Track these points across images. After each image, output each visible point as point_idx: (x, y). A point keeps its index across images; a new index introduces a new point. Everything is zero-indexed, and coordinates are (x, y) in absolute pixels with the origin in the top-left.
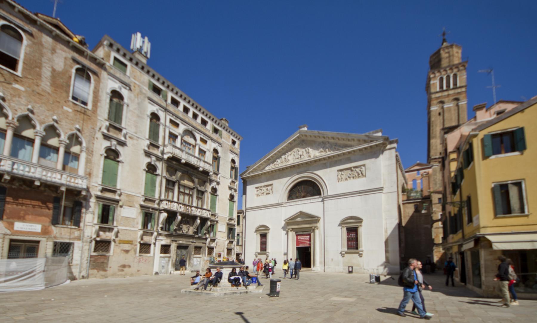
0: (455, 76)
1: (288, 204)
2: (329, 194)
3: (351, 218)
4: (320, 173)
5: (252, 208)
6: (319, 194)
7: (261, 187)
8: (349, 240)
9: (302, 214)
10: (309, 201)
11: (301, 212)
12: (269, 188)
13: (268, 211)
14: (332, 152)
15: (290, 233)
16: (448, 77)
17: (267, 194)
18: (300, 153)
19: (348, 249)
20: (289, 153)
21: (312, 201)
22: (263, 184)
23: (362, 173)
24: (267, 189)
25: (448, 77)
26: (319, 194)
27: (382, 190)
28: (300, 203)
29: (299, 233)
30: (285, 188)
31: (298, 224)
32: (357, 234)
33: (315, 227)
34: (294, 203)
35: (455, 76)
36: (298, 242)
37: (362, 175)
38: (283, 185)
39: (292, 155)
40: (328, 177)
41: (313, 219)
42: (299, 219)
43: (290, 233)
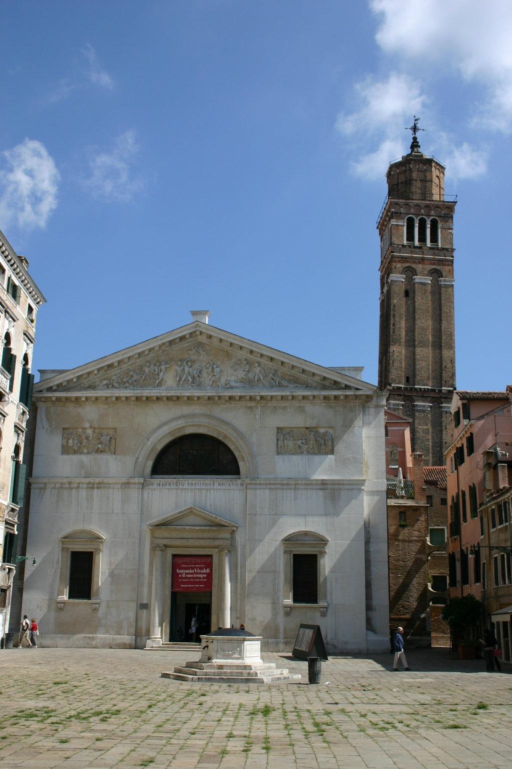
15: (158, 553)
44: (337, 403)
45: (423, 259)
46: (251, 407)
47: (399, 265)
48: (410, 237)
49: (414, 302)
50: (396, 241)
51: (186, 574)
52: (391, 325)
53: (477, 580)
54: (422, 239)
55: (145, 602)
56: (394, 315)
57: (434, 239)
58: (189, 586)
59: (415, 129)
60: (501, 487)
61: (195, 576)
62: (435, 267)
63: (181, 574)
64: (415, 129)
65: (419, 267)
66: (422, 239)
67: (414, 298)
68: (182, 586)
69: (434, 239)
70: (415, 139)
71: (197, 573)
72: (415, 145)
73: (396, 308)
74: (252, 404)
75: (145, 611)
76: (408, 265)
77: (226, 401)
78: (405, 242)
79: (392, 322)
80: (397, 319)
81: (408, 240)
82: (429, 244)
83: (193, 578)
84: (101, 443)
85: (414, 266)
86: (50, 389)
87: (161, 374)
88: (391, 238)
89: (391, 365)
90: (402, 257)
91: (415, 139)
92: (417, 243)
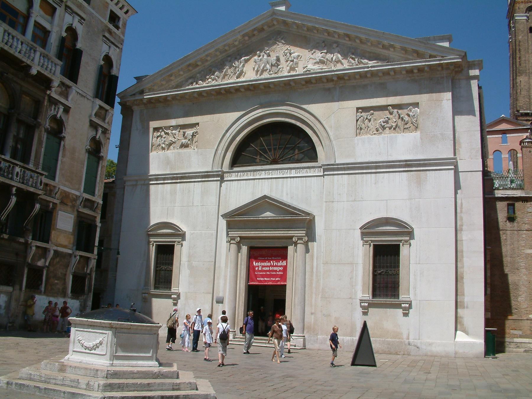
2: (337, 162)
3: (387, 221)
4: (318, 109)
7: (168, 128)
9: (265, 202)
11: (265, 197)
12: (189, 132)
14: (354, 62)
21: (293, 173)
22: (173, 122)
28: (263, 175)
31: (256, 228)
37: (414, 126)
38: (223, 127)
44: (422, 76)
46: (329, 90)
51: (263, 266)
52: (517, 58)
56: (520, 50)
58: (265, 279)
61: (271, 268)
63: (258, 267)
68: (3, 218)
71: (273, 266)
73: (521, 44)
74: (330, 85)
75: (220, 305)
77: (303, 85)
79: (518, 56)
80: (523, 53)
83: (269, 271)
89: (519, 93)
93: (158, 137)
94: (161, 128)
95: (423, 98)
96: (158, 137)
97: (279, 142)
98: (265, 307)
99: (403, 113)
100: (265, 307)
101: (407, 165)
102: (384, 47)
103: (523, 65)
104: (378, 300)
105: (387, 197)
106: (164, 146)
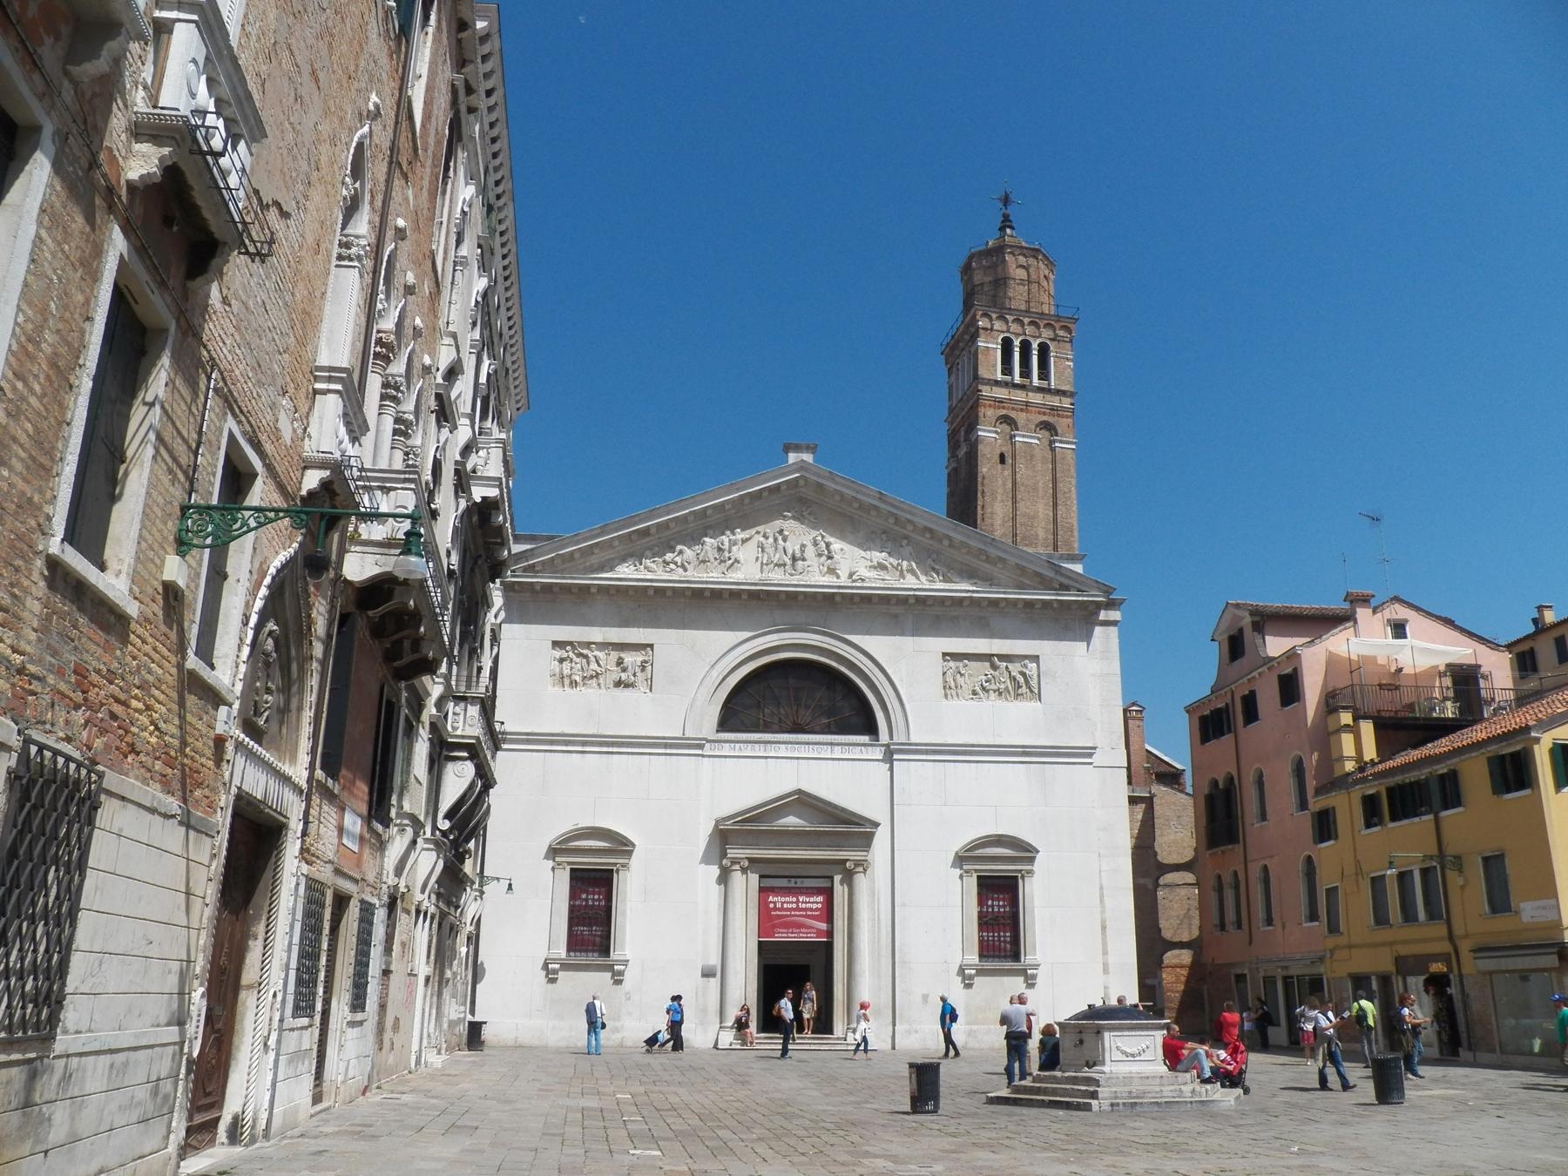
0: (1044, 350)
1: (726, 750)
2: (914, 739)
3: (999, 840)
4: (881, 646)
5: (530, 739)
6: (871, 728)
7: (588, 645)
8: (986, 922)
9: (803, 801)
10: (826, 752)
11: (799, 792)
12: (631, 659)
13: (622, 763)
16: (1026, 347)
17: (618, 684)
18: (792, 546)
19: (981, 956)
20: (740, 535)
21: (837, 752)
22: (597, 634)
23: (1027, 682)
24: (620, 662)
25: (1026, 347)
26: (871, 728)
27: (1090, 755)
28: (783, 751)
29: (775, 879)
30: (717, 674)
31: (780, 846)
32: (1014, 902)
33: (858, 863)
34: (759, 750)
35: (1044, 350)
36: (767, 919)
38: (707, 659)
39: (753, 544)
40: (907, 669)
41: (849, 830)
42: (791, 821)
43: (738, 879)
45: (1027, 404)
46: (896, 616)
47: (990, 412)
48: (1007, 368)
49: (1014, 473)
50: (983, 372)
53: (1432, 915)
54: (1026, 372)
55: (714, 960)
57: (1044, 374)
59: (1006, 201)
60: (1367, 758)
62: (1045, 418)
64: (1006, 201)
65: (1021, 418)
66: (1026, 372)
67: (1013, 466)
69: (1044, 374)
70: (1006, 218)
72: (1006, 222)
76: (1004, 412)
78: (999, 376)
81: (1003, 373)
82: (1036, 381)
84: (624, 670)
85: (1013, 414)
86: (531, 569)
87: (734, 548)
88: (976, 369)
90: (995, 400)
91: (1006, 218)
92: (1017, 379)
93: (561, 660)
94: (571, 643)
95: (1043, 648)
96: (561, 660)
97: (801, 694)
98: (795, 981)
99: (1015, 668)
100: (795, 981)
101: (1026, 753)
102: (988, 560)
103: (988, 521)
104: (989, 965)
105: (997, 802)
106: (578, 678)
